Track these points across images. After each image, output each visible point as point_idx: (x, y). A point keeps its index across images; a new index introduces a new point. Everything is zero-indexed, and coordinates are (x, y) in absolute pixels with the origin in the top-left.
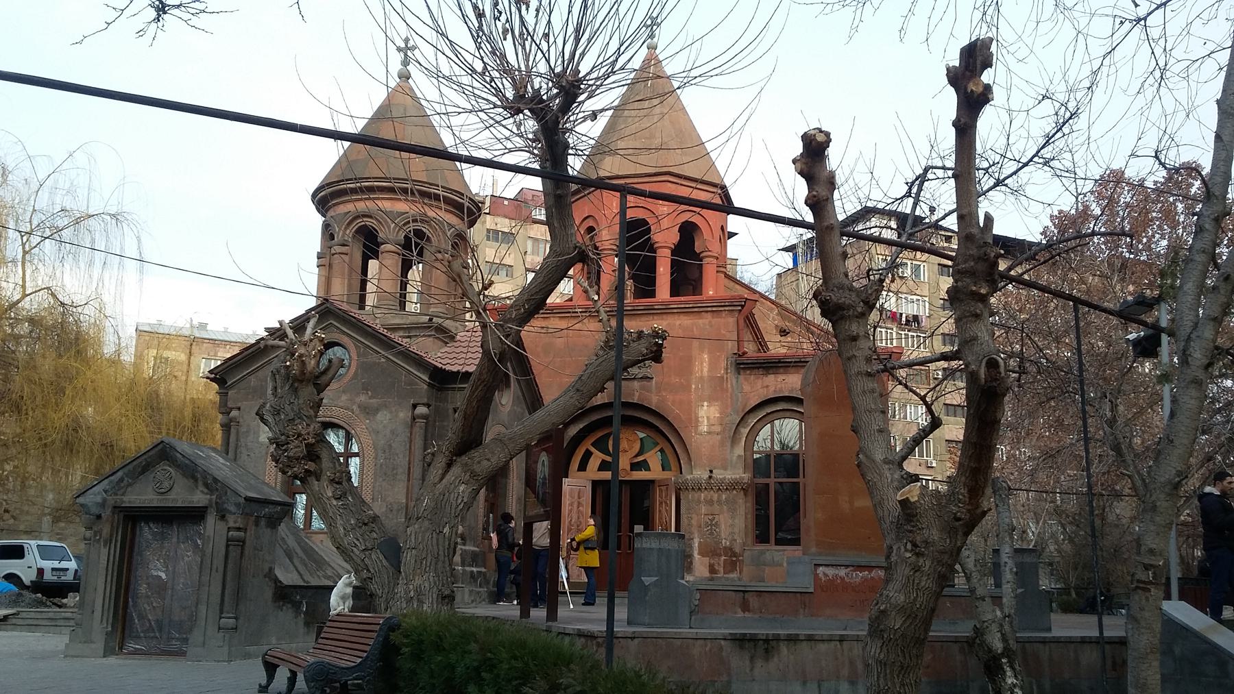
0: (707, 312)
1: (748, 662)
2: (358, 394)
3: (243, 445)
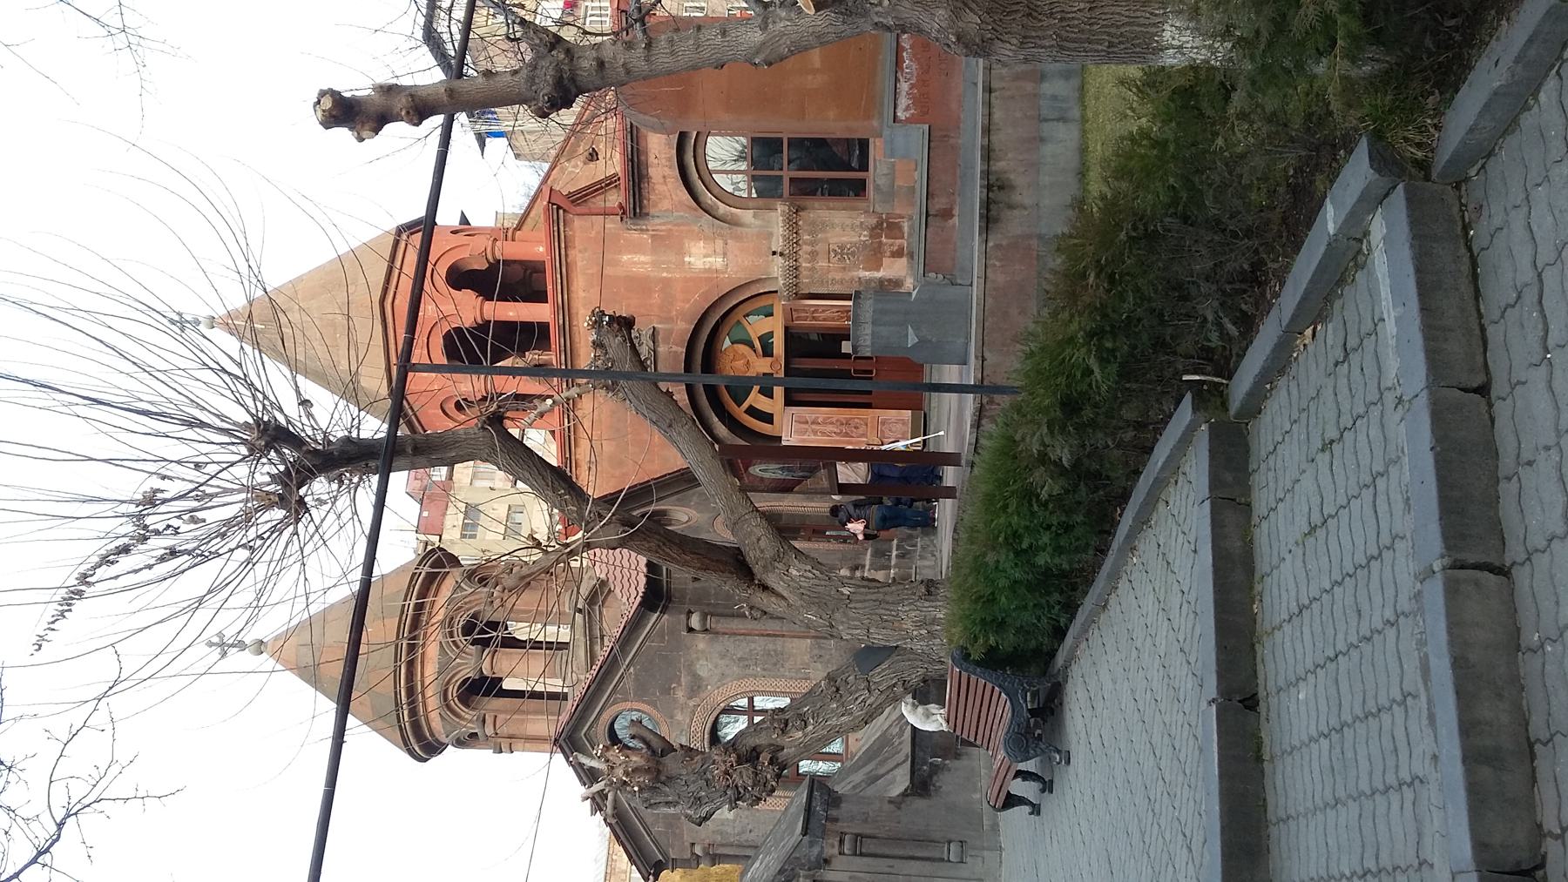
0: (566, 255)
1: (1016, 212)
2: (675, 700)
3: (737, 838)
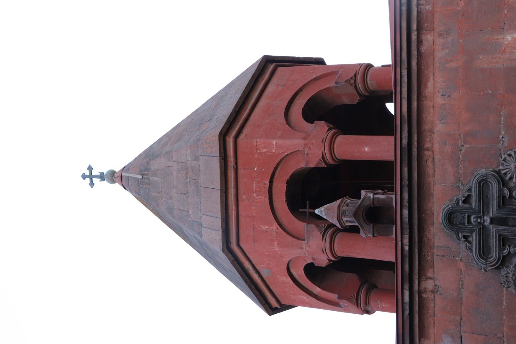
0: (419, 42)
